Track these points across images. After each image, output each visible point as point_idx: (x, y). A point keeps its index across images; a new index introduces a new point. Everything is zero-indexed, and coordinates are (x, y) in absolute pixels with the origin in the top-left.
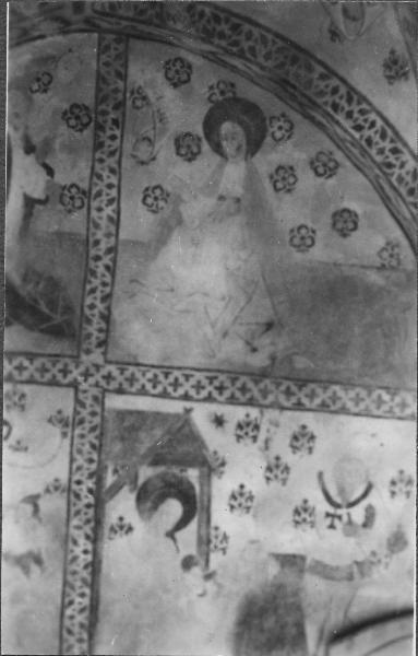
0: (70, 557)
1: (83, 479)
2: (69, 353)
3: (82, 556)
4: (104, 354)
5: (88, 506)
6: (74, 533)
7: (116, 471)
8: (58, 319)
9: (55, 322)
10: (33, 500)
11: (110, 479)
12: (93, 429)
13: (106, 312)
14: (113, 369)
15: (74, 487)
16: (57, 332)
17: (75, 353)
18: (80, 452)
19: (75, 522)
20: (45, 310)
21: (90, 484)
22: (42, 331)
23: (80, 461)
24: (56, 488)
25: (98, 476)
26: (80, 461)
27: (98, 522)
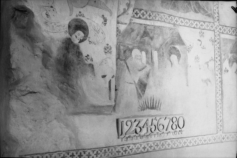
0: (216, 80)
1: (218, 57)
2: (212, 22)
3: (219, 79)
4: (219, 22)
5: (219, 65)
6: (217, 72)
7: (224, 55)
8: (209, 12)
9: (209, 13)
10: (207, 63)
11: (223, 57)
12: (218, 43)
13: (218, 12)
14: (221, 27)
15: (216, 59)
16: (209, 16)
17: (213, 22)
18: (216, 49)
19: (216, 69)
20: (207, 10)
21: (219, 58)
22: (206, 15)
23: (216, 52)
24: (212, 60)
25: (220, 56)
26: (216, 52)
27: (221, 69)
